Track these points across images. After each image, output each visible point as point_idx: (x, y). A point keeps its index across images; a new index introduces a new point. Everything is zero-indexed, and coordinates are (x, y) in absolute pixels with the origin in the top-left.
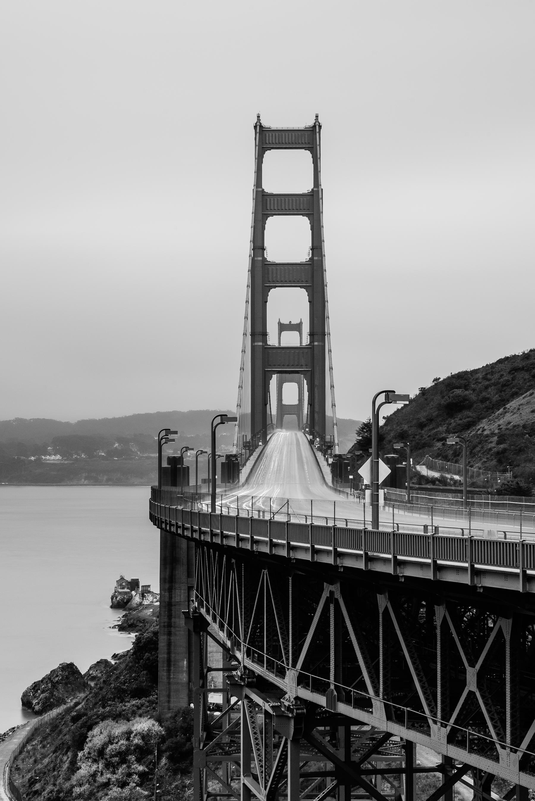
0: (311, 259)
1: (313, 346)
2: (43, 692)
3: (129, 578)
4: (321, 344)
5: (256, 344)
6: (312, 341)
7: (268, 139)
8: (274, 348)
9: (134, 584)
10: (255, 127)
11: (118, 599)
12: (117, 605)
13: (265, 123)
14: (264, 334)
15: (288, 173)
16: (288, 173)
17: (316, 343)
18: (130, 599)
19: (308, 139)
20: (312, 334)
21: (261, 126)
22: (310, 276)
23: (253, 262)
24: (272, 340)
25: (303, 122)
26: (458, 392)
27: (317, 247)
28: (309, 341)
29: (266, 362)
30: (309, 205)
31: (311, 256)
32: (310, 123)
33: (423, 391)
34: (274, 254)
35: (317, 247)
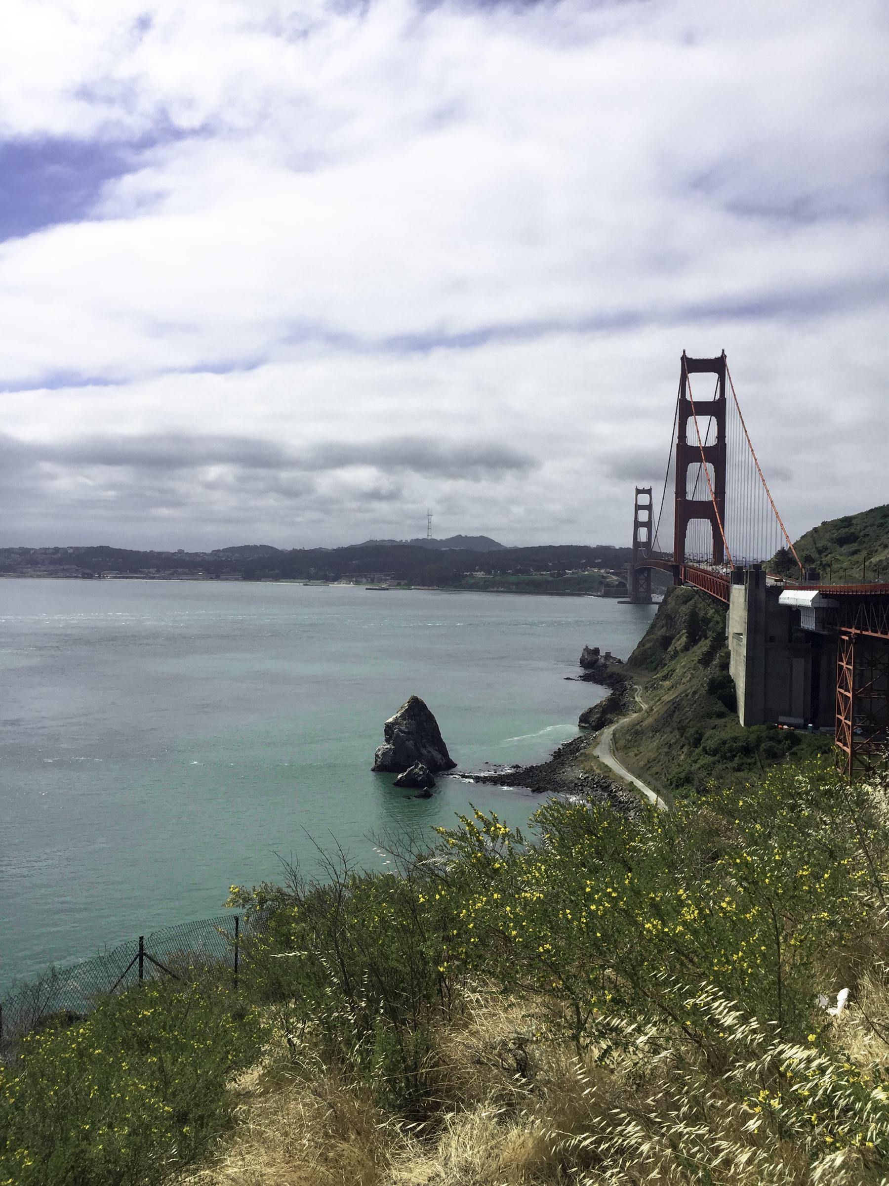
7: (690, 365)
9: (596, 651)
10: (682, 358)
12: (584, 663)
13: (689, 355)
15: (703, 387)
16: (703, 387)
18: (597, 660)
19: (718, 366)
21: (687, 358)
25: (715, 354)
26: (844, 530)
29: (686, 510)
30: (716, 409)
32: (719, 355)
33: (815, 529)
34: (692, 440)
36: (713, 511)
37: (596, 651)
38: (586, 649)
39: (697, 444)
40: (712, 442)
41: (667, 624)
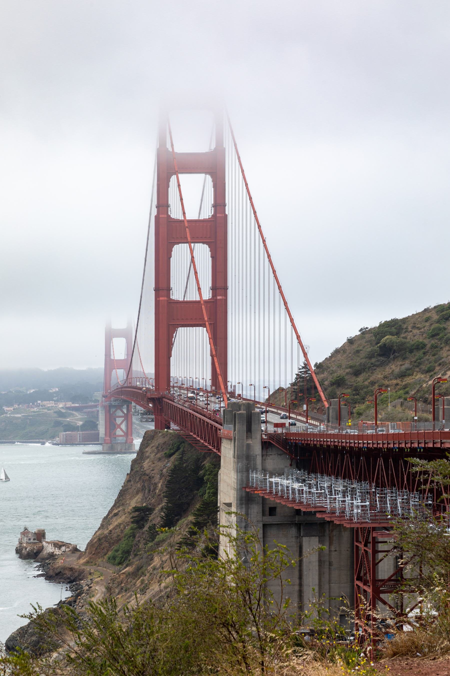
0: (214, 216)
1: (216, 299)
2: (32, 635)
3: (33, 529)
4: (224, 298)
5: (161, 299)
6: (214, 295)
8: (178, 302)
9: (40, 535)
11: (27, 550)
14: (169, 289)
17: (219, 298)
18: (41, 549)
20: (214, 289)
22: (213, 232)
23: (157, 218)
24: (177, 294)
27: (219, 204)
28: (211, 295)
29: (170, 316)
31: (213, 213)
35: (219, 204)
36: (212, 315)
37: (40, 535)
38: (25, 532)
39: (181, 218)
40: (207, 213)
41: (143, 489)
